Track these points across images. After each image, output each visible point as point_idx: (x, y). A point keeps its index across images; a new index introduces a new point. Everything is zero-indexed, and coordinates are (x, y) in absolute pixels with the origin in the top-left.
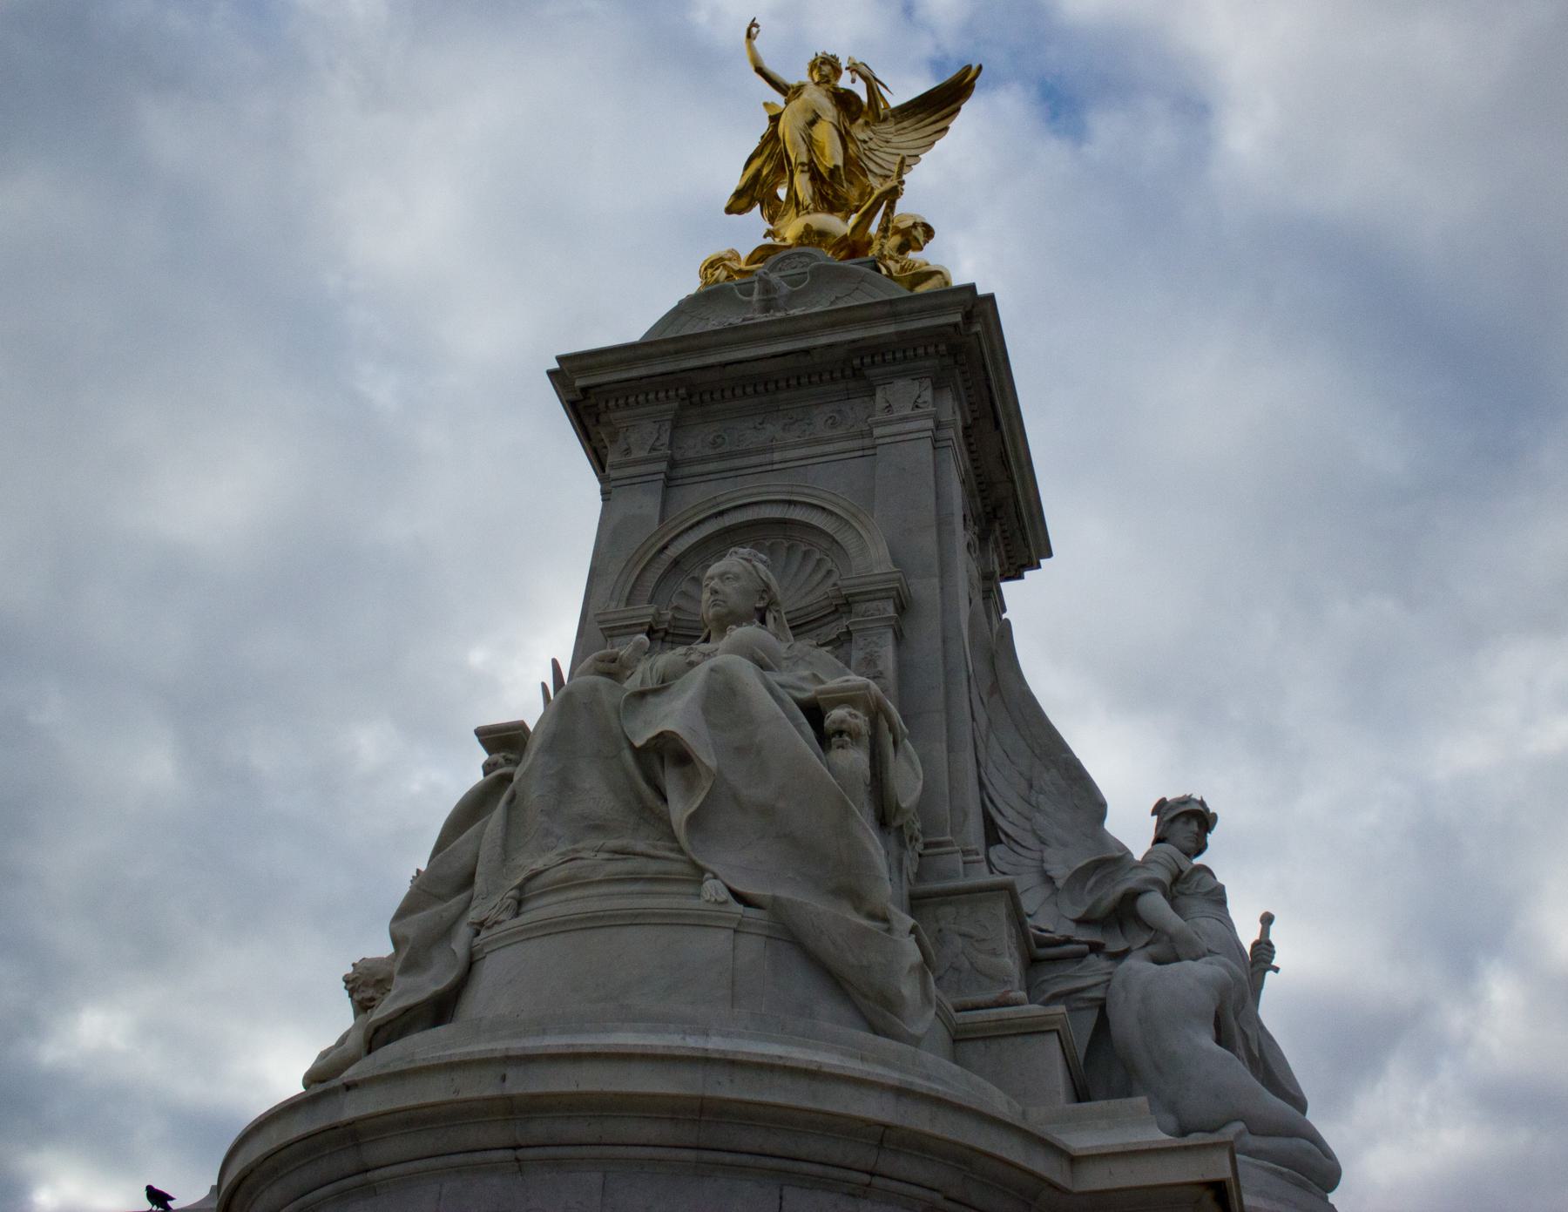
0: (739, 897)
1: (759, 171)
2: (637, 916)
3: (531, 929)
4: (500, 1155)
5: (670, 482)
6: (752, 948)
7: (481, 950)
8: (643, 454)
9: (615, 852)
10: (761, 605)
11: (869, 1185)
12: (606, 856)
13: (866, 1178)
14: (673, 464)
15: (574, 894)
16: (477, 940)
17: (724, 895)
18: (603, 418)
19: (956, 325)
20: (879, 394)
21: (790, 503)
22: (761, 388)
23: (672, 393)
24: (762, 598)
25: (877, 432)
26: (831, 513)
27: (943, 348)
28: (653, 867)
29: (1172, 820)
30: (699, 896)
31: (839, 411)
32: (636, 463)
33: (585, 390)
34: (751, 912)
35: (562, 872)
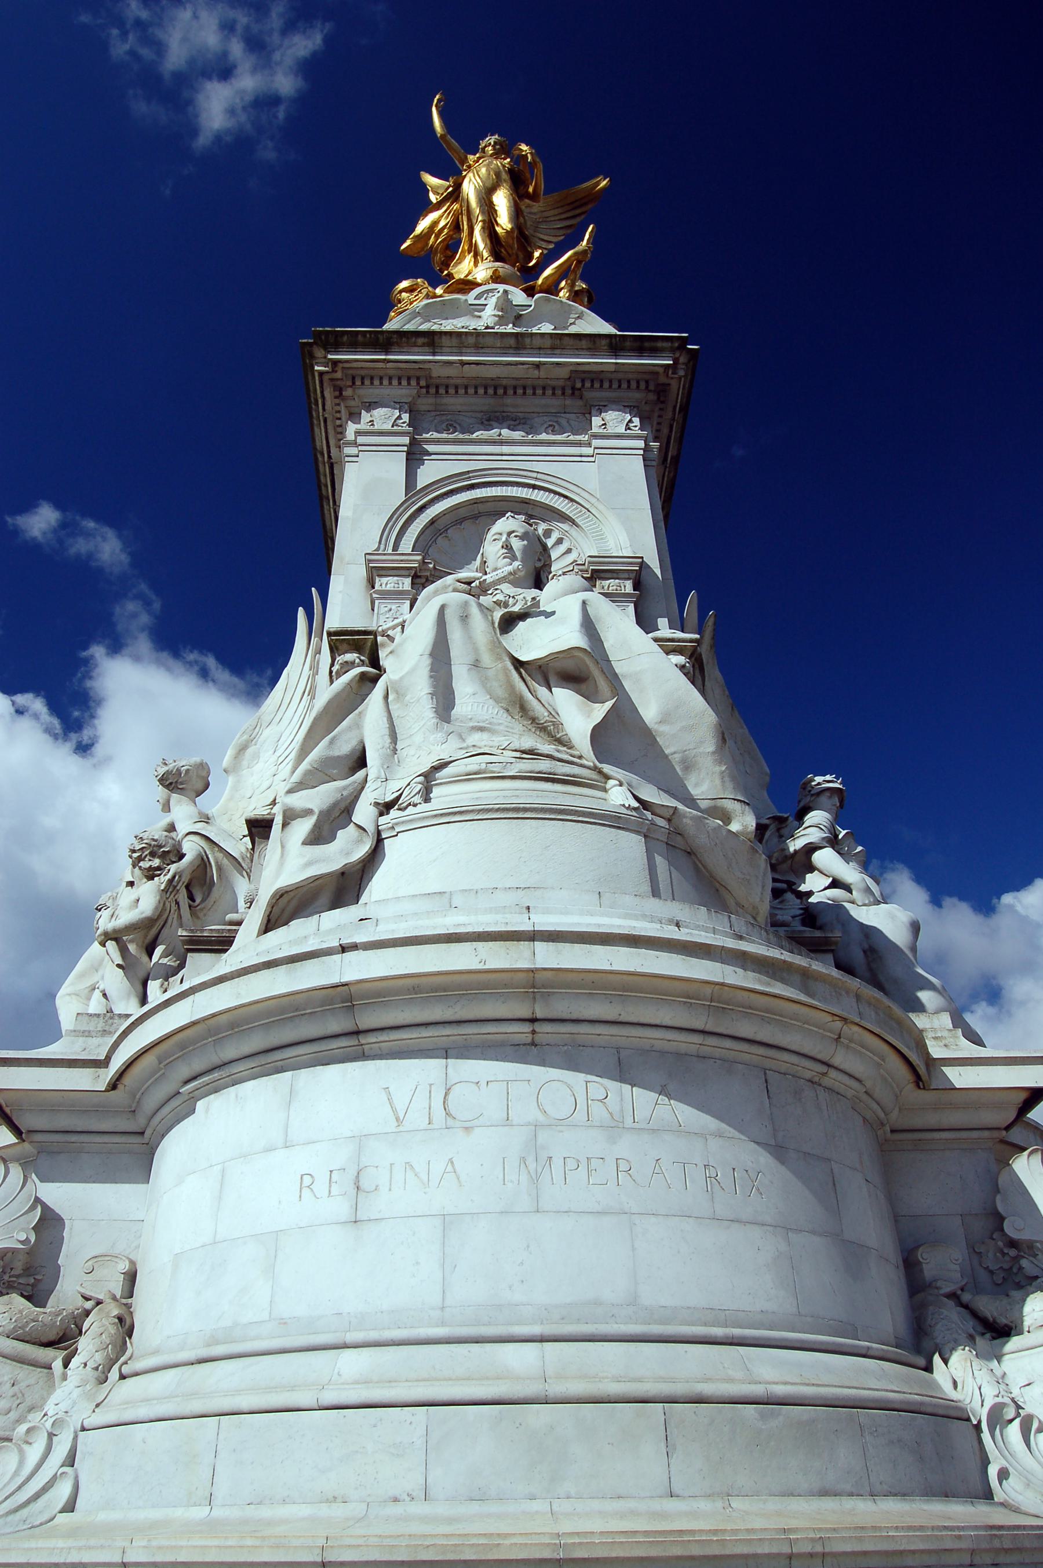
0: (644, 804)
1: (435, 223)
7: (393, 828)
8: (388, 426)
9: (523, 752)
10: (539, 565)
11: (824, 1074)
12: (518, 754)
16: (383, 820)
17: (636, 804)
18: (348, 392)
22: (491, 391)
23: (413, 382)
24: (539, 560)
27: (652, 387)
31: (557, 422)
32: (381, 433)
33: (335, 363)
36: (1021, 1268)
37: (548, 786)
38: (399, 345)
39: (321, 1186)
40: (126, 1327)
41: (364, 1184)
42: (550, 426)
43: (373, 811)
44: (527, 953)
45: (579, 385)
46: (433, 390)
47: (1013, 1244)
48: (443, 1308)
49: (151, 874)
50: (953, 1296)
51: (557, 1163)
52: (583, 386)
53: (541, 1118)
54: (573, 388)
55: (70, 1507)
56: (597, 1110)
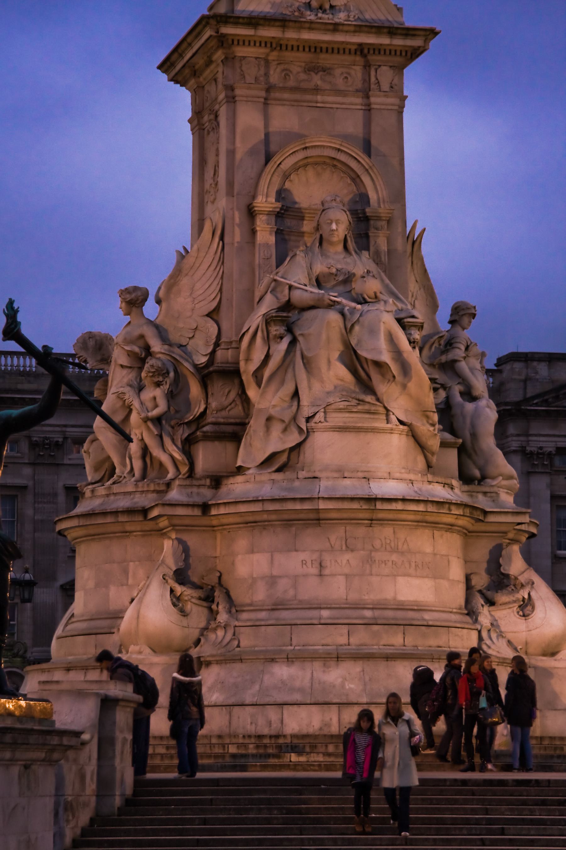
0: (401, 422)
2: (373, 429)
3: (336, 428)
4: (366, 522)
5: (266, 103)
6: (404, 438)
10: (346, 233)
12: (357, 402)
13: (451, 527)
14: (268, 90)
15: (347, 415)
16: (308, 425)
17: (398, 423)
19: (419, 47)
20: (373, 73)
21: (339, 150)
25: (373, 100)
26: (359, 161)
28: (373, 408)
29: (463, 315)
30: (388, 421)
34: (405, 427)
35: (342, 405)
36: (504, 582)
37: (367, 416)
38: (263, 25)
39: (309, 564)
40: (228, 594)
41: (323, 564)
42: (346, 78)
43: (304, 420)
44: (373, 504)
45: (366, 51)
46: (279, 48)
47: (503, 574)
48: (347, 599)
49: (158, 384)
50: (480, 592)
51: (377, 562)
52: (369, 52)
53: (372, 548)
54: (362, 51)
55: (238, 646)
56: (388, 547)
